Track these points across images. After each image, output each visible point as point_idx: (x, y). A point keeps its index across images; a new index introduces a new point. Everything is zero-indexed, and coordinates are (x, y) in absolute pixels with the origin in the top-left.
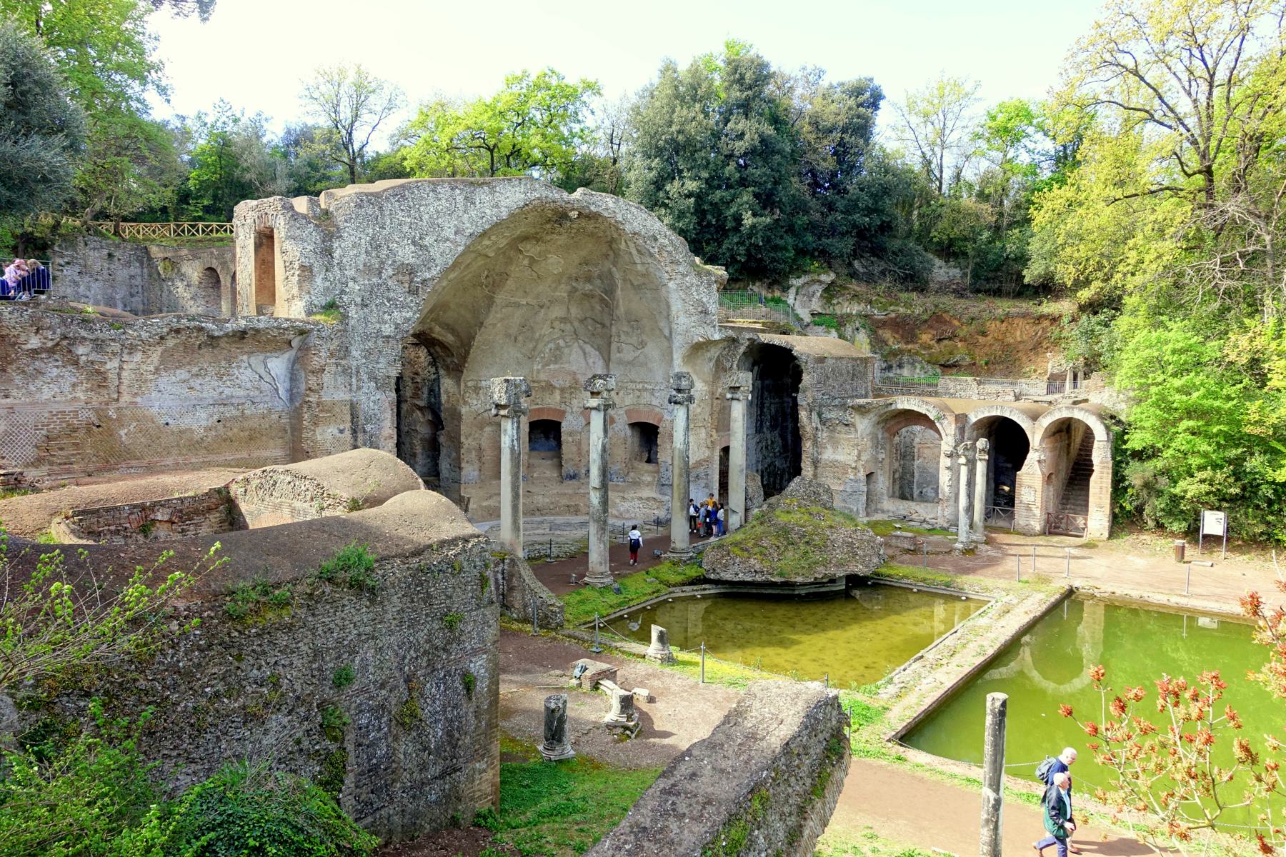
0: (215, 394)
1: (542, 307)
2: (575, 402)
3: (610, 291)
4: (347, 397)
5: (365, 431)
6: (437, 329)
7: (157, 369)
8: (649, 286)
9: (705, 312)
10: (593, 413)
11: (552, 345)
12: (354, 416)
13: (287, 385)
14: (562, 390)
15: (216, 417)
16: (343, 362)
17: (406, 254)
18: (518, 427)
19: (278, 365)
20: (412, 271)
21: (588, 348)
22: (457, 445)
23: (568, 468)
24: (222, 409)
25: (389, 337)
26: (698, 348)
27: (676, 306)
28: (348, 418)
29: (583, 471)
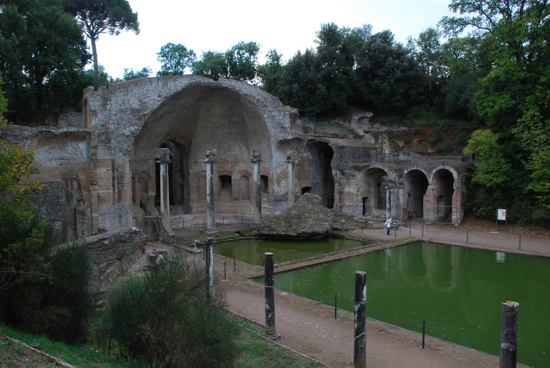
0: (59, 155)
1: (218, 128)
2: (237, 167)
3: (244, 120)
4: (110, 158)
5: (118, 171)
6: (178, 138)
7: (37, 146)
8: (257, 117)
9: (283, 127)
10: (207, 164)
11: (227, 144)
12: (113, 165)
13: (86, 153)
14: (232, 163)
15: (59, 163)
16: (108, 145)
17: (136, 105)
18: (166, 168)
19: (82, 146)
20: (138, 111)
21: (241, 145)
22: (189, 185)
23: (235, 195)
24: (62, 161)
25: (128, 136)
26: (283, 144)
27: (269, 125)
28: (111, 166)
29: (241, 197)
